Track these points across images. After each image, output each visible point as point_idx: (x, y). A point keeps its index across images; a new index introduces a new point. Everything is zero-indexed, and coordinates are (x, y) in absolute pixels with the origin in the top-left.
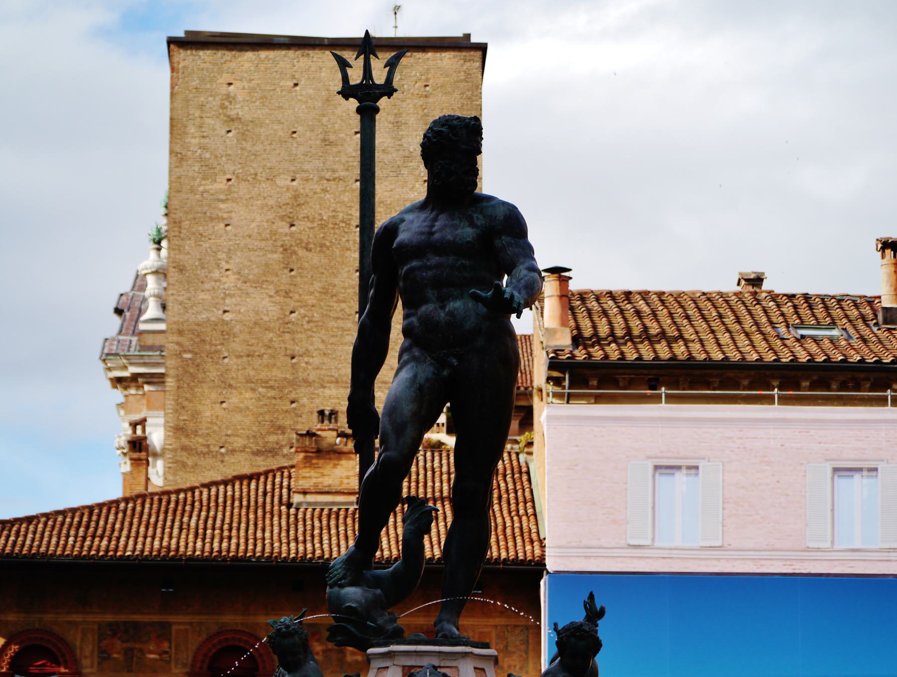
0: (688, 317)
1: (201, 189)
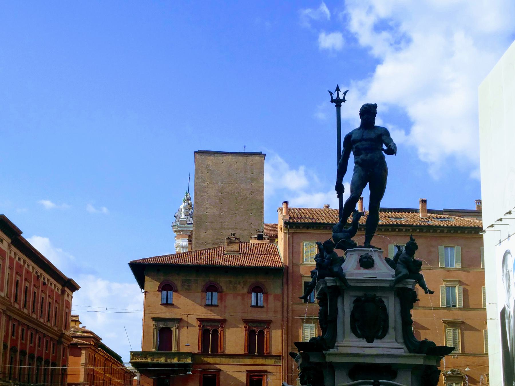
0: (314, 214)
1: (202, 185)
